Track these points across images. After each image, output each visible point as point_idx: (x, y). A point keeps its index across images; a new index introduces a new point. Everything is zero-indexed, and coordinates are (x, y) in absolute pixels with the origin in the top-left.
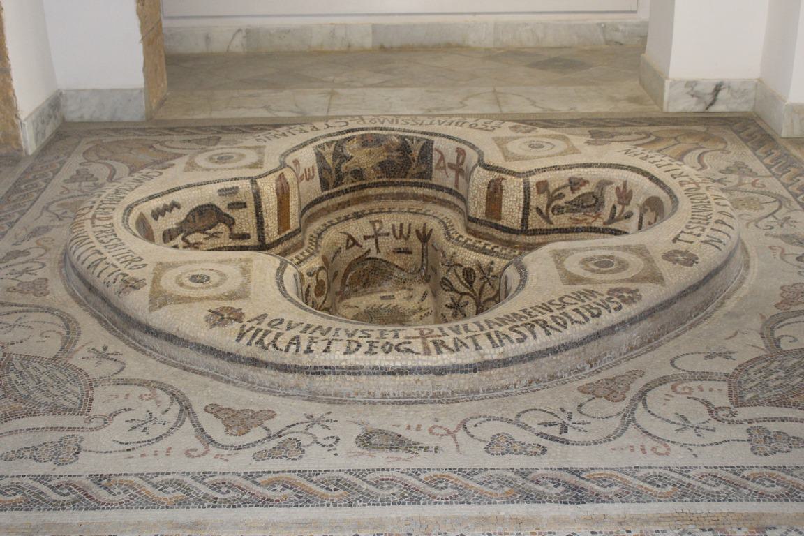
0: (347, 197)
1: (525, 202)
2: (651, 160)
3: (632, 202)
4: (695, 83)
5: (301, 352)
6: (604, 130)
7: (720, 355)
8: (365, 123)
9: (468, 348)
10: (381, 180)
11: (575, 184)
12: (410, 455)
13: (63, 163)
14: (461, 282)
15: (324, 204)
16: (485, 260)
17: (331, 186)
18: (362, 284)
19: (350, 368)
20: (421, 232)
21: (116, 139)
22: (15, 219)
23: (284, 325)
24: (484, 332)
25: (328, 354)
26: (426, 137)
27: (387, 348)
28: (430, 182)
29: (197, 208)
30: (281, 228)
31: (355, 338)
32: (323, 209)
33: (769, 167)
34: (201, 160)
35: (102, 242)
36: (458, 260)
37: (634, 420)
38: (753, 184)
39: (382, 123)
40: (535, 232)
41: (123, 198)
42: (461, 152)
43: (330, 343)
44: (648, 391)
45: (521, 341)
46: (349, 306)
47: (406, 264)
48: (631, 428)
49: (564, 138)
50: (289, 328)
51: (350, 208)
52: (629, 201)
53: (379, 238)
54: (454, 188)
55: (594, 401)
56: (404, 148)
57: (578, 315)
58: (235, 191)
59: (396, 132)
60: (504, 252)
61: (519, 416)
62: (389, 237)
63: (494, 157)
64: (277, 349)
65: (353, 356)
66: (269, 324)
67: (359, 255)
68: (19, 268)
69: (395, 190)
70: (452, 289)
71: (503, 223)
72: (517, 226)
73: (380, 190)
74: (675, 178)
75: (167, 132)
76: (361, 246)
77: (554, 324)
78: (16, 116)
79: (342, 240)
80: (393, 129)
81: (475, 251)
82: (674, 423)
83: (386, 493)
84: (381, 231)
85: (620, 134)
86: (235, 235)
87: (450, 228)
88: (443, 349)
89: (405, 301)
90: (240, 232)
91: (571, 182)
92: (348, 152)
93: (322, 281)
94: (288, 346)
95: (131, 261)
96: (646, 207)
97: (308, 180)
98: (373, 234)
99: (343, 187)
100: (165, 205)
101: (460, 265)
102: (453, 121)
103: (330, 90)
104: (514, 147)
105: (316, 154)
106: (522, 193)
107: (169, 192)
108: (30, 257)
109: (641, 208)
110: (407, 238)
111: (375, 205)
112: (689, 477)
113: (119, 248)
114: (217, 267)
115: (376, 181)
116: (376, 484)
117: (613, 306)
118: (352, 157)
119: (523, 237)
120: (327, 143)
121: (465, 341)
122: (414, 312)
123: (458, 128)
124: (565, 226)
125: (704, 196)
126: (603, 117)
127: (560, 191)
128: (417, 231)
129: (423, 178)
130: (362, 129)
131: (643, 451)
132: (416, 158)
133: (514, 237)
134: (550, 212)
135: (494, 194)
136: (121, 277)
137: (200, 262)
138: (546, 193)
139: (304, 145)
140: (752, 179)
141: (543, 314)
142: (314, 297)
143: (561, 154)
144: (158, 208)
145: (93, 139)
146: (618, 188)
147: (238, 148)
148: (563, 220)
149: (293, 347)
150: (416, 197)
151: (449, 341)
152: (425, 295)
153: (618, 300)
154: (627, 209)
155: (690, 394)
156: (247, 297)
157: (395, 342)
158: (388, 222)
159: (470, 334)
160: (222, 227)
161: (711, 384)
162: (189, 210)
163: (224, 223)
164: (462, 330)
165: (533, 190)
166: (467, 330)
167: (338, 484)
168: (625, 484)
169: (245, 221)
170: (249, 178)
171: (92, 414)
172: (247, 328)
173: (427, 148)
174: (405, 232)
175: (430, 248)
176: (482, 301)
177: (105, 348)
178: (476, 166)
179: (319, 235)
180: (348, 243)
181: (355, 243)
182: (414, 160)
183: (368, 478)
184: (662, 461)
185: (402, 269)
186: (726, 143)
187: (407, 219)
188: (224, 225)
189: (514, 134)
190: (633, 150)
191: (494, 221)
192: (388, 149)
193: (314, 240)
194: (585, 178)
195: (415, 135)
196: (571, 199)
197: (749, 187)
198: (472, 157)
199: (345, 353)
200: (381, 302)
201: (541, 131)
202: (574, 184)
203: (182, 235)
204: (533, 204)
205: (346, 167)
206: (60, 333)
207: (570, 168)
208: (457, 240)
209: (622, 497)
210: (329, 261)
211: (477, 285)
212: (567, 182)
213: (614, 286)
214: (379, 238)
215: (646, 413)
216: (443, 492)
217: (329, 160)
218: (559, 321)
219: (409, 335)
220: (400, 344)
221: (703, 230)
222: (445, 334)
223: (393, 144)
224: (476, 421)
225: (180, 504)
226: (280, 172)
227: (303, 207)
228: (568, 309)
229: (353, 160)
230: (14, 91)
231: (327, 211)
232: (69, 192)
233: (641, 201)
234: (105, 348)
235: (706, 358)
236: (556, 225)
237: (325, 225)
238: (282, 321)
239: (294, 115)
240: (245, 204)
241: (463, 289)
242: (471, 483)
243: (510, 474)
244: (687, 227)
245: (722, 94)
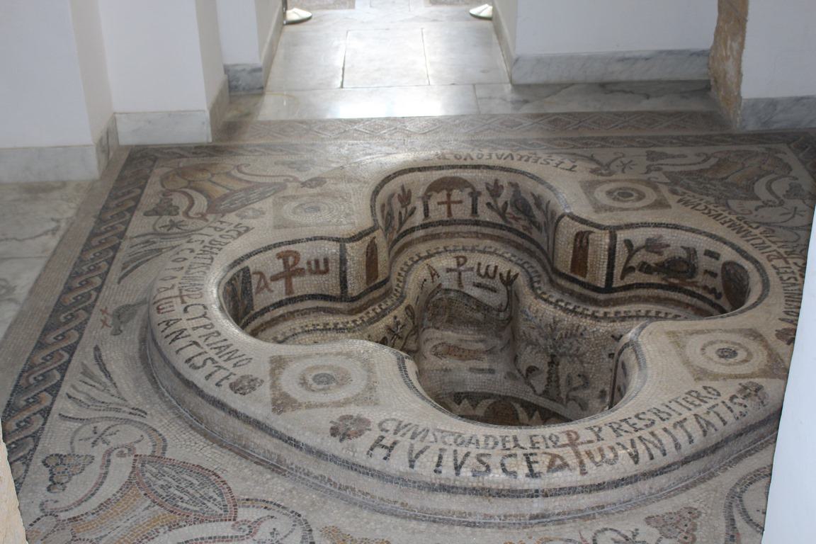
3: (413, 199)
52: (410, 200)
109: (423, 198)
154: (409, 208)
182: (239, 301)
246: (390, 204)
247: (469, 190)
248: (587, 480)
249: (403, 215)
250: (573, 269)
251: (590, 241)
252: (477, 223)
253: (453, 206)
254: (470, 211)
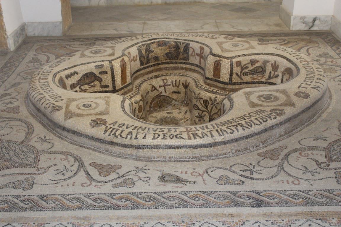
0: (152, 69)
1: (231, 70)
2: (287, 51)
3: (278, 70)
4: (305, 17)
5: (133, 139)
6: (264, 38)
7: (320, 138)
8: (159, 36)
9: (208, 136)
10: (166, 61)
11: (253, 62)
12: (182, 185)
13: (26, 54)
14: (203, 106)
15: (141, 72)
16: (213, 96)
17: (144, 64)
18: (158, 107)
19: (155, 146)
20: (184, 84)
21: (49, 44)
22: (5, 79)
23: (125, 127)
24: (215, 129)
25: (145, 139)
26: (186, 42)
27: (172, 136)
28: (188, 62)
29: (85, 74)
30: (123, 83)
31: (157, 132)
32: (141, 74)
33: (338, 54)
34: (87, 53)
35: (43, 89)
36: (201, 96)
37: (283, 168)
38: (332, 62)
39: (167, 36)
40: (235, 84)
41: (52, 70)
42: (202, 49)
43: (146, 134)
44: (289, 155)
45: (231, 133)
46: (153, 117)
47: (178, 98)
48: (282, 172)
49: (247, 42)
50: (127, 128)
51: (153, 74)
52: (277, 70)
53: (166, 87)
54: (199, 64)
55: (265, 160)
56: (177, 47)
57: (257, 121)
58: (102, 66)
59: (173, 40)
60: (221, 92)
61: (231, 167)
62: (170, 86)
63: (217, 50)
64: (122, 137)
65: (156, 140)
66: (118, 126)
67: (157, 94)
68: (6, 101)
69: (173, 65)
70: (199, 109)
71: (221, 80)
72: (227, 81)
73: (166, 66)
74: (298, 59)
75: (72, 40)
76: (158, 90)
77: (246, 126)
78: (5, 34)
79: (149, 88)
80: (172, 39)
81: (209, 92)
82: (301, 170)
83: (172, 203)
84: (167, 84)
85: (272, 40)
86: (103, 86)
87: (197, 82)
88: (197, 137)
89: (178, 114)
90: (105, 85)
91: (251, 61)
92: (152, 49)
93: (141, 106)
94: (127, 136)
95: (56, 98)
96: (285, 72)
97: (134, 61)
98: (163, 85)
99: (150, 64)
100: (71, 73)
101: (202, 99)
102: (198, 35)
103: (143, 22)
104: (226, 46)
105: (138, 50)
106: (229, 67)
107: (73, 67)
108: (12, 96)
110: (178, 87)
111: (164, 72)
112: (309, 195)
113: (51, 92)
114: (94, 100)
115: (164, 61)
116: (168, 198)
117: (272, 117)
118: (154, 51)
119: (230, 86)
120: (143, 45)
121: (206, 133)
122: (182, 119)
123: (201, 38)
124: (249, 81)
125: (311, 67)
126: (264, 33)
127: (246, 66)
128: (183, 83)
129: (185, 60)
130: (158, 39)
131: (288, 182)
132: (182, 51)
133: (226, 86)
134: (242, 75)
135: (217, 67)
136: (52, 105)
137: (87, 98)
138: (240, 66)
139: (133, 46)
140: (331, 60)
141: (241, 121)
142: (138, 113)
143: (247, 49)
144: (68, 74)
145: (40, 44)
146: (272, 64)
147: (104, 47)
148: (248, 78)
149: (129, 137)
150: (182, 68)
151: (199, 133)
152: (186, 112)
153: (275, 114)
154: (276, 73)
155: (308, 156)
156: (108, 114)
157: (175, 134)
158: (170, 80)
159: (209, 130)
160: (97, 82)
161: (317, 152)
162: (82, 75)
163: (98, 80)
164: (205, 128)
165: (234, 65)
166: (207, 128)
167: (151, 199)
168: (280, 198)
169: (107, 79)
170: (108, 60)
171: (39, 167)
172: (108, 128)
173: (187, 47)
174: (177, 84)
175: (188, 91)
176: (212, 114)
177: (45, 137)
178: (209, 54)
179: (140, 85)
180: (152, 89)
181: (155, 89)
182: (181, 52)
183: (164, 196)
184: (297, 187)
185: (176, 100)
186: (319, 44)
187: (178, 78)
188: (98, 82)
189: (225, 40)
190: (278, 47)
191: (217, 79)
192: (170, 47)
193: (137, 88)
194: (258, 60)
195: (181, 41)
196: (251, 69)
197: (330, 63)
198: (207, 50)
199: (153, 139)
200: (167, 115)
201: (237, 39)
202: (253, 62)
203: (79, 86)
204: (234, 71)
205: (151, 56)
206: (25, 130)
207: (251, 55)
208: (201, 87)
209: (279, 204)
210: (144, 97)
211: (209, 107)
212: (249, 61)
213: (273, 108)
214: (166, 87)
215: (289, 165)
216: (198, 202)
217: (144, 52)
218: (249, 124)
219: (181, 131)
220: (177, 135)
221: (312, 82)
222: (197, 130)
223: (172, 45)
224: (212, 169)
225: (79, 208)
226: (122, 58)
227: (132, 73)
228: (253, 118)
229: (154, 52)
230: (4, 23)
231: (143, 75)
232: (29, 67)
233: (283, 70)
234: (45, 137)
235: (314, 140)
236: (245, 81)
237: (142, 81)
238: (124, 125)
239: (128, 33)
240: (107, 72)
241: (203, 109)
242: (211, 198)
243: (228, 194)
244: (304, 81)
245: (316, 22)
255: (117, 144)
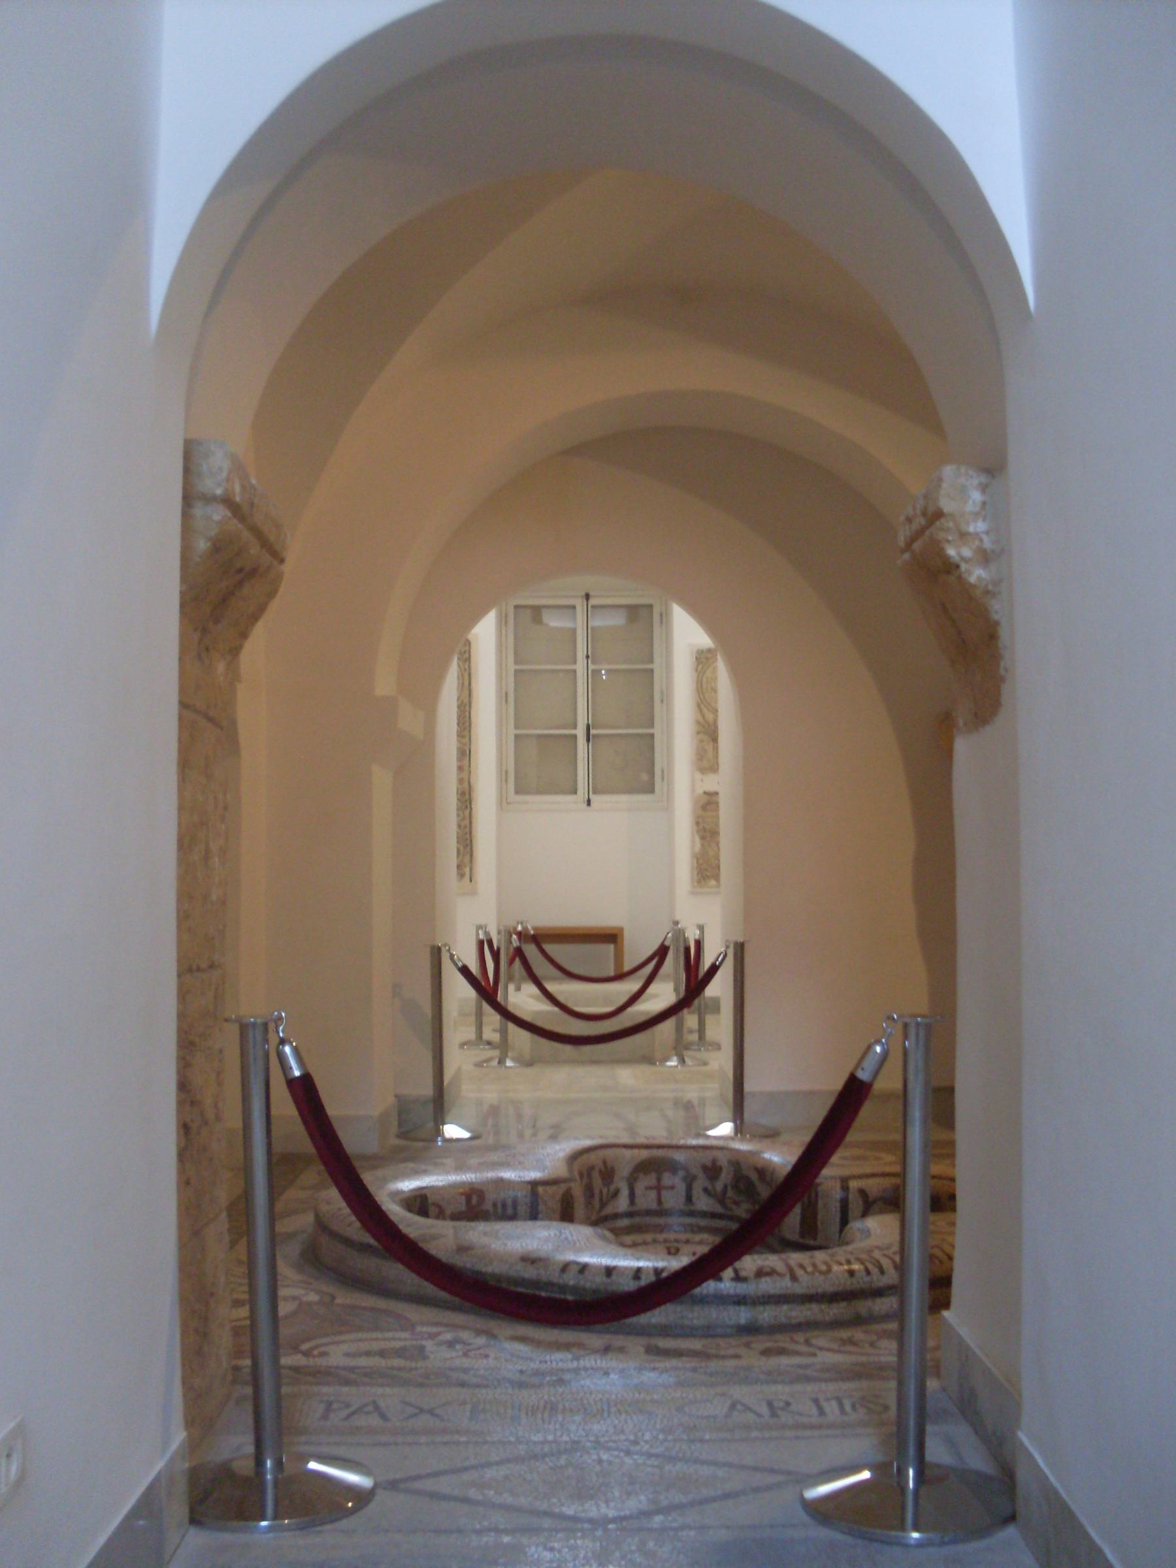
3: (616, 1179)
154: (612, 1188)
246: (589, 1176)
247: (681, 1173)
248: (798, 1289)
249: (604, 1195)
250: (802, 1235)
251: (820, 1194)
252: (691, 1214)
253: (664, 1193)
254: (682, 1199)
255: (724, 1465)
